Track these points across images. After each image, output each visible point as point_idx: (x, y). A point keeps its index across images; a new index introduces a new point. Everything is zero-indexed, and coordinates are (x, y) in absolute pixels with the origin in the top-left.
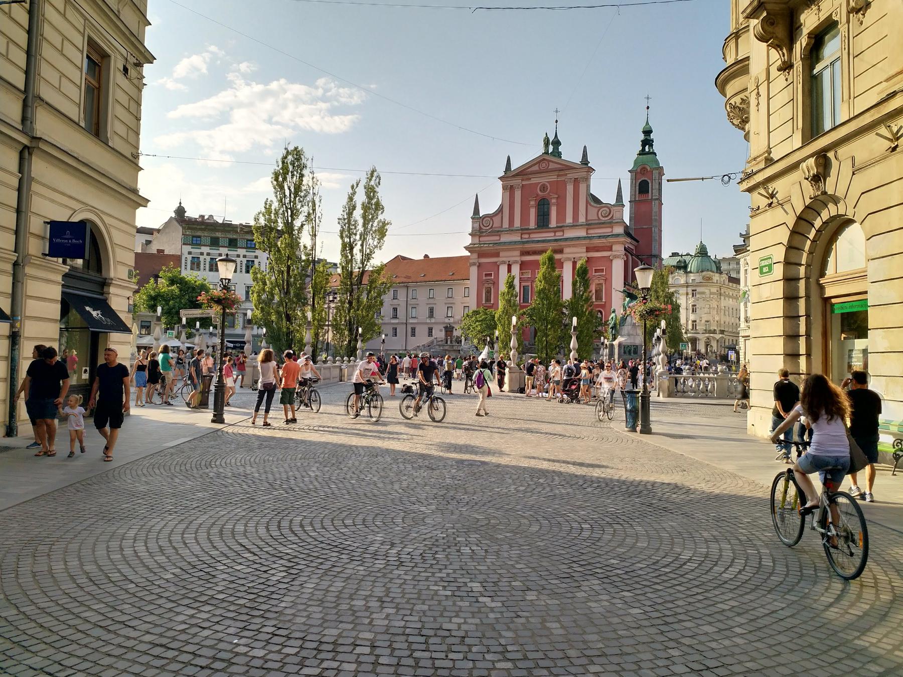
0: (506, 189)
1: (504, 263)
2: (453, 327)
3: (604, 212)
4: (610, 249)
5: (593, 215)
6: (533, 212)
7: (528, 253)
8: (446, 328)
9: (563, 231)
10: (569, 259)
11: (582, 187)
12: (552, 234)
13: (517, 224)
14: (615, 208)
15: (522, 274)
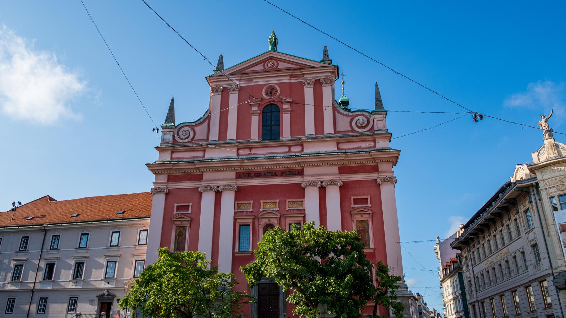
0: (217, 91)
1: (209, 188)
2: (113, 297)
3: (361, 121)
4: (375, 169)
5: (344, 124)
6: (255, 121)
7: (248, 175)
8: (100, 297)
9: (302, 146)
10: (313, 184)
11: (326, 91)
12: (286, 149)
13: (232, 134)
14: (376, 116)
15: (237, 206)
